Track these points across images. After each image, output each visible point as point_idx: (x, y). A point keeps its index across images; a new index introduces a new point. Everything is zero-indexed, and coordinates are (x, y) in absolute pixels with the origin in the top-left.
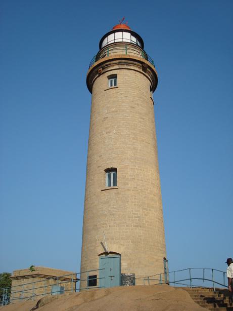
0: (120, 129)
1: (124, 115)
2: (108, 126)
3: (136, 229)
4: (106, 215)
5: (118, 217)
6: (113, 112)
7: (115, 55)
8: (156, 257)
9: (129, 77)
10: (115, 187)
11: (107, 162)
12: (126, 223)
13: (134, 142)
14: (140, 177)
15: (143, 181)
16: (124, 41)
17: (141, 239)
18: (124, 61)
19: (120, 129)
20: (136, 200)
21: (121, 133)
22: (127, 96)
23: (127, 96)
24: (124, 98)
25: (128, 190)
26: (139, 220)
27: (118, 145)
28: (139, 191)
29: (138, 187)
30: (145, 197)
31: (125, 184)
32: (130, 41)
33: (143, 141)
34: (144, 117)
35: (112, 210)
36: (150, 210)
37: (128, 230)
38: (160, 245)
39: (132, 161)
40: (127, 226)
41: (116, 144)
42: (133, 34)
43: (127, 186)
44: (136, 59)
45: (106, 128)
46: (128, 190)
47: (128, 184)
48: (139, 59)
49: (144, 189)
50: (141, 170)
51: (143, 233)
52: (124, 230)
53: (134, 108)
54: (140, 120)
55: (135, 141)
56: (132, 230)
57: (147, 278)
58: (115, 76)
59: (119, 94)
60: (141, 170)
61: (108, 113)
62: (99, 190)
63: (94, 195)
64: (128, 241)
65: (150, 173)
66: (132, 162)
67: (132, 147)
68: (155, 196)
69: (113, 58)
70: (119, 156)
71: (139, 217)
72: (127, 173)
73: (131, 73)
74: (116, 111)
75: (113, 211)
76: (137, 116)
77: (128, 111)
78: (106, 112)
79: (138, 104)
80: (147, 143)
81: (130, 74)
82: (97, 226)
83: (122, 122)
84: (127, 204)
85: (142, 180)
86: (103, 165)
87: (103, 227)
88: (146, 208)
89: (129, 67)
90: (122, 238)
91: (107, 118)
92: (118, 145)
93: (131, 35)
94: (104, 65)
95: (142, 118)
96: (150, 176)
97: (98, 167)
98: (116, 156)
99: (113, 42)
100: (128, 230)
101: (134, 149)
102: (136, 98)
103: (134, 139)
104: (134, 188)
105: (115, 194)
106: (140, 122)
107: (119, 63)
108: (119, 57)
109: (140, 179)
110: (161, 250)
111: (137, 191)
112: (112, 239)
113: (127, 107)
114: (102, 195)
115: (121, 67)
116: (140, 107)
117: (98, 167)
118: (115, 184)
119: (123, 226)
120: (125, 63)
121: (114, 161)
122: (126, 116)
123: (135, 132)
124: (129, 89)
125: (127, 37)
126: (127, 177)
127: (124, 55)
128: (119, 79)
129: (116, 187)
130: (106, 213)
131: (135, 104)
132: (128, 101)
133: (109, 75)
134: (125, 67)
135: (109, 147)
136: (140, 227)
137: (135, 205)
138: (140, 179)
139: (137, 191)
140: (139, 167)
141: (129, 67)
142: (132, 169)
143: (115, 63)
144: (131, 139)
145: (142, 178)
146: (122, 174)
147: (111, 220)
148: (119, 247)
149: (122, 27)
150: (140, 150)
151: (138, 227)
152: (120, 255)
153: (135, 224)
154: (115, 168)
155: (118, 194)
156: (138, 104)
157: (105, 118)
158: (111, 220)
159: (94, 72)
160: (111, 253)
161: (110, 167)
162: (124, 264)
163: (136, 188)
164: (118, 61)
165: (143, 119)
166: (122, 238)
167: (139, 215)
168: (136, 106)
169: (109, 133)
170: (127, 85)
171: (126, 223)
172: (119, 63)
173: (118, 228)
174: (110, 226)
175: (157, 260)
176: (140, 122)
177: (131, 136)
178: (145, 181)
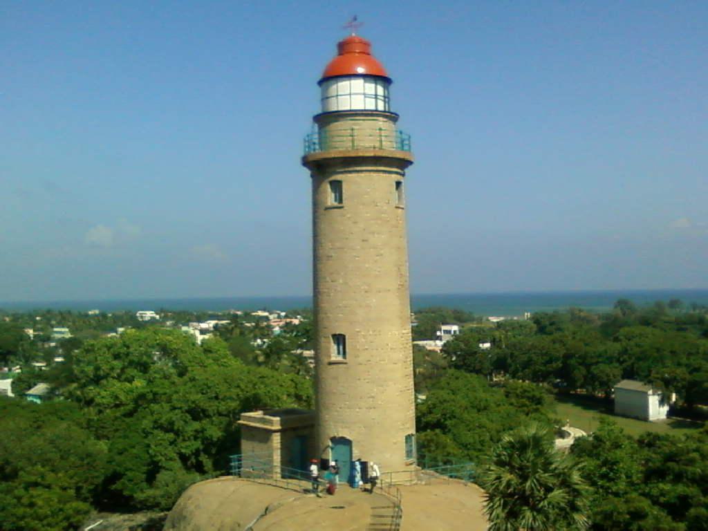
26: (373, 401)
31: (357, 356)
47: (358, 356)
48: (372, 155)
53: (366, 241)
72: (358, 342)
74: (343, 248)
78: (331, 247)
79: (373, 233)
91: (331, 256)
115: (347, 169)
116: (376, 236)
118: (344, 353)
126: (358, 347)
128: (344, 186)
129: (345, 361)
156: (373, 233)
167: (373, 395)
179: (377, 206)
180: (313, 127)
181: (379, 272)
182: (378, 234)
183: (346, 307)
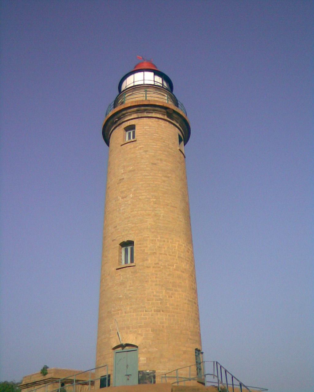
0: (138, 192)
1: (144, 174)
2: (124, 189)
3: (157, 314)
4: (120, 299)
5: (134, 300)
6: (130, 171)
7: (132, 102)
8: (184, 349)
9: (150, 126)
10: (133, 264)
11: (123, 234)
12: (145, 307)
13: (155, 208)
14: (163, 249)
15: (166, 255)
16: (146, 82)
17: (163, 327)
18: (143, 108)
19: (138, 192)
20: (158, 279)
21: (140, 197)
22: (147, 151)
23: (147, 151)
24: (143, 153)
25: (148, 267)
26: (161, 303)
27: (136, 212)
28: (162, 267)
29: (160, 263)
30: (169, 275)
32: (152, 83)
33: (168, 205)
34: (170, 175)
35: (128, 292)
36: (175, 291)
37: (147, 317)
38: (190, 333)
39: (153, 230)
40: (146, 311)
41: (133, 211)
42: (157, 73)
43: (146, 262)
44: (157, 104)
45: (122, 192)
46: (148, 267)
47: (147, 260)
48: (161, 104)
49: (168, 265)
50: (164, 241)
51: (166, 319)
52: (142, 316)
53: (155, 164)
54: (164, 179)
55: (156, 206)
56: (152, 315)
57: (164, 376)
58: (132, 127)
59: (137, 148)
60: (164, 241)
61: (123, 174)
62: (114, 269)
63: (109, 275)
64: (148, 329)
65: (177, 245)
66: (153, 232)
67: (153, 213)
68: (183, 272)
69: (129, 105)
70: (137, 225)
71: (160, 299)
72: (146, 247)
73: (152, 122)
74: (134, 170)
75: (130, 294)
76: (160, 175)
77: (148, 169)
78: (123, 172)
79: (161, 160)
80: (173, 207)
81: (151, 123)
82: (111, 312)
83: (141, 183)
84: (146, 285)
85: (165, 254)
86: (118, 238)
87: (118, 314)
88: (171, 287)
89: (150, 115)
90: (140, 327)
91: (123, 179)
92: (136, 212)
93: (155, 74)
94: (120, 114)
95: (166, 177)
96: (177, 248)
97: (113, 241)
98: (133, 226)
99: (132, 85)
100: (146, 316)
101: (155, 215)
102: (159, 152)
103: (155, 203)
104: (155, 264)
105: (132, 272)
106: (164, 181)
107: (138, 110)
108: (136, 104)
109: (163, 252)
110: (190, 339)
111: (159, 267)
112: (128, 328)
113: (147, 164)
114: (117, 275)
115: (140, 115)
116: (164, 163)
117: (113, 241)
118: (132, 261)
119: (141, 311)
120: (145, 111)
121: (131, 232)
122: (145, 175)
123: (157, 194)
124: (150, 141)
125: (149, 78)
126: (146, 252)
127: (143, 101)
130: (121, 296)
131: (158, 160)
132: (147, 156)
133: (128, 125)
134: (145, 114)
135: (125, 215)
136: (163, 311)
137: (156, 285)
138: (163, 252)
139: (159, 267)
140: (161, 238)
141: (150, 115)
142: (153, 240)
143: (133, 112)
144: (152, 204)
145: (165, 251)
146: (140, 247)
147: (127, 304)
148: (136, 338)
149: (145, 66)
150: (163, 217)
151: (160, 311)
152: (137, 347)
153: (156, 308)
154: (133, 241)
155: (135, 272)
156: (161, 160)
157: (120, 180)
158: (127, 304)
159: (109, 124)
160: (127, 345)
161: (125, 240)
162: (142, 359)
163: (158, 264)
164: (135, 109)
165: (168, 177)
166: (140, 327)
167: (161, 298)
168: (159, 162)
169: (125, 197)
170: (146, 137)
171: (145, 307)
172: (137, 112)
173: (135, 314)
174: (125, 313)
175: (185, 352)
176: (164, 181)
177: (152, 200)
178: (170, 255)
179: (164, 142)
180: (113, 102)
181: (167, 189)
182: (165, 161)
183: (135, 216)
